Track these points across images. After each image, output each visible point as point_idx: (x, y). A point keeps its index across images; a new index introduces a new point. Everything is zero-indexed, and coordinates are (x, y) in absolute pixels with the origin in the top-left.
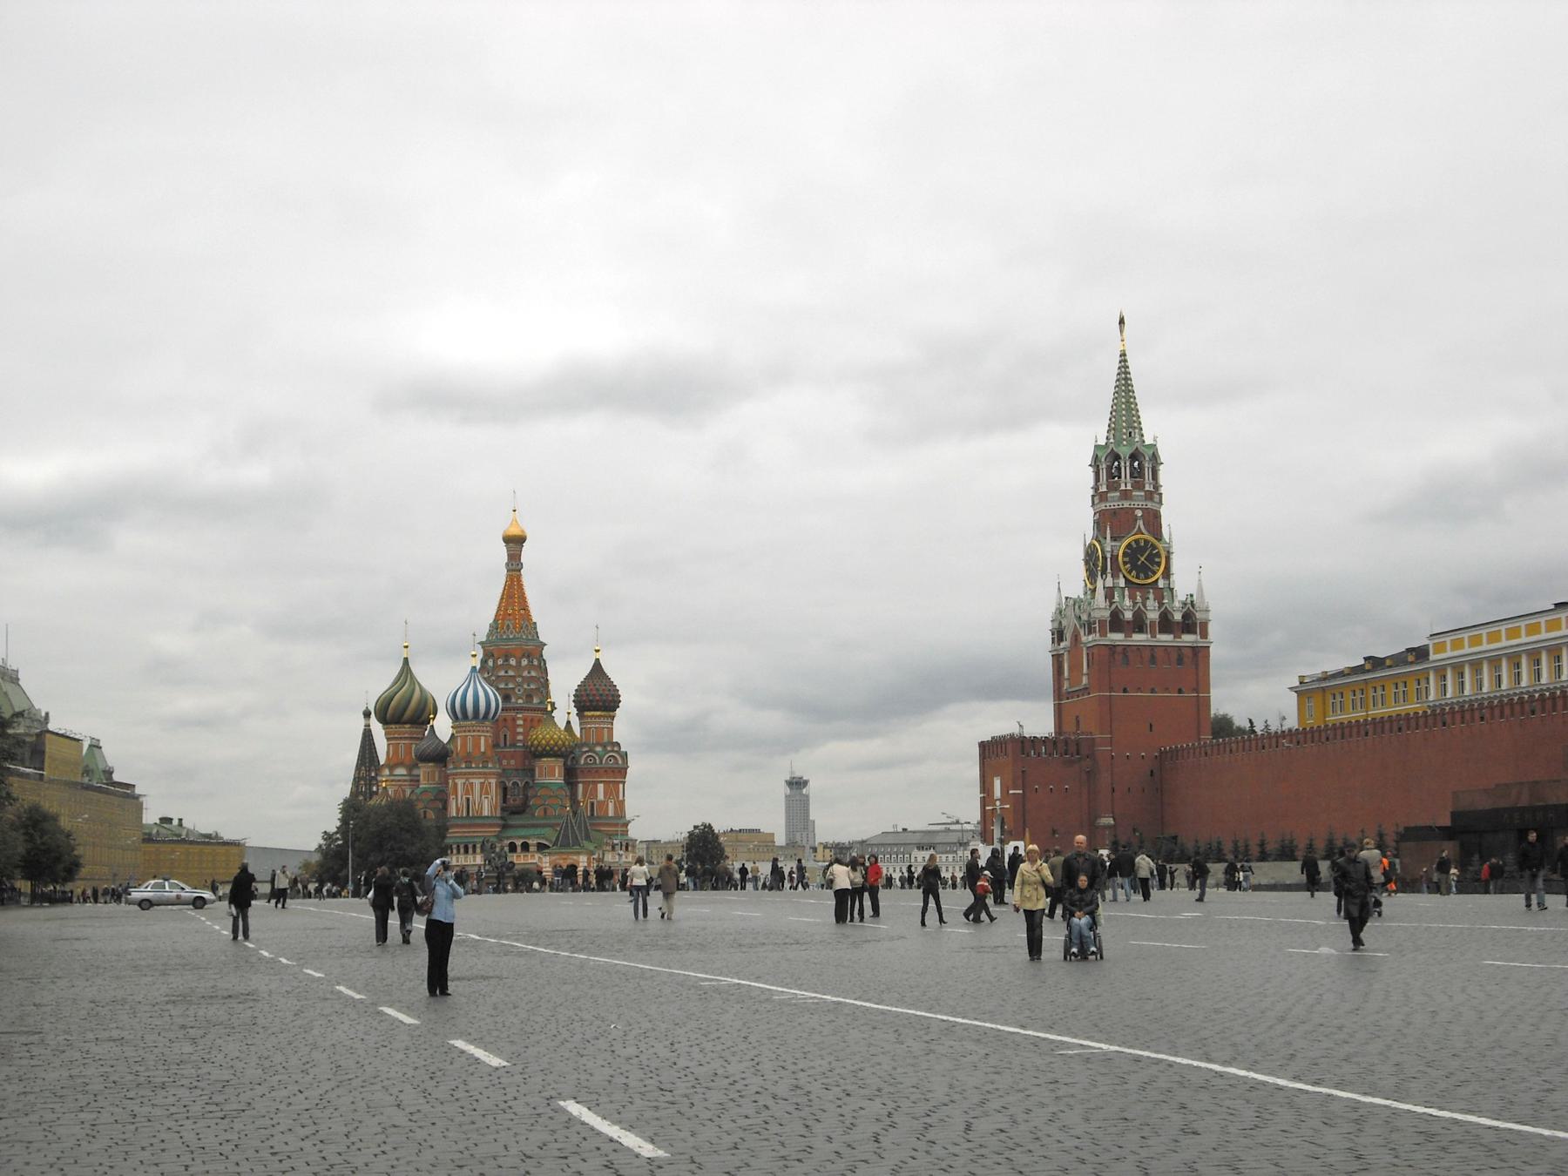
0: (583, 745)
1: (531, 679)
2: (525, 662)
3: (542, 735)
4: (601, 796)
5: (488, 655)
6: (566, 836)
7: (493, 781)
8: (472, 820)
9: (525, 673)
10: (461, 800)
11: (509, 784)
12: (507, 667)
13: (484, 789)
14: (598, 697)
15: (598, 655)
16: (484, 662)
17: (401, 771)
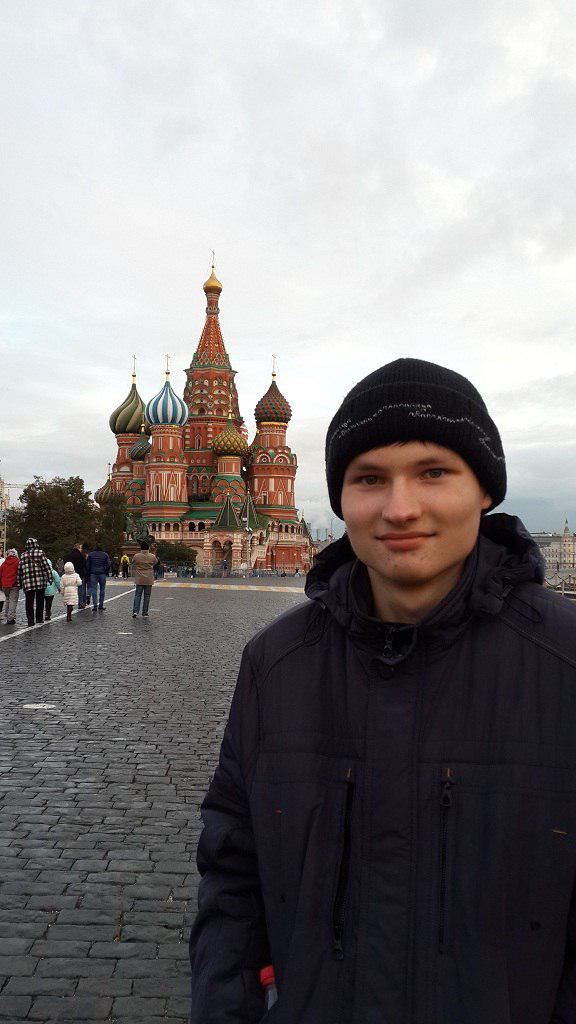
0: (260, 448)
1: (221, 397)
2: (215, 384)
3: (228, 438)
4: (272, 489)
5: (190, 379)
6: (224, 518)
7: (180, 474)
8: (162, 504)
9: (216, 392)
10: (153, 487)
11: (201, 479)
12: (202, 387)
13: (171, 480)
14: (274, 410)
15: (276, 379)
16: (187, 384)
17: (126, 469)
